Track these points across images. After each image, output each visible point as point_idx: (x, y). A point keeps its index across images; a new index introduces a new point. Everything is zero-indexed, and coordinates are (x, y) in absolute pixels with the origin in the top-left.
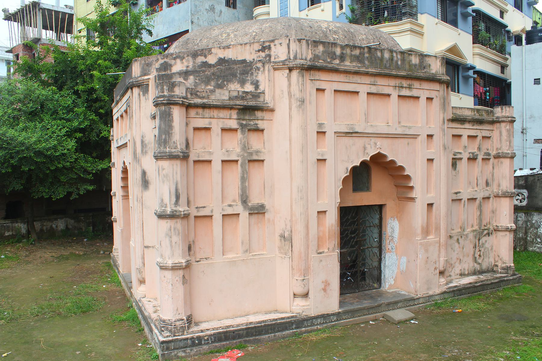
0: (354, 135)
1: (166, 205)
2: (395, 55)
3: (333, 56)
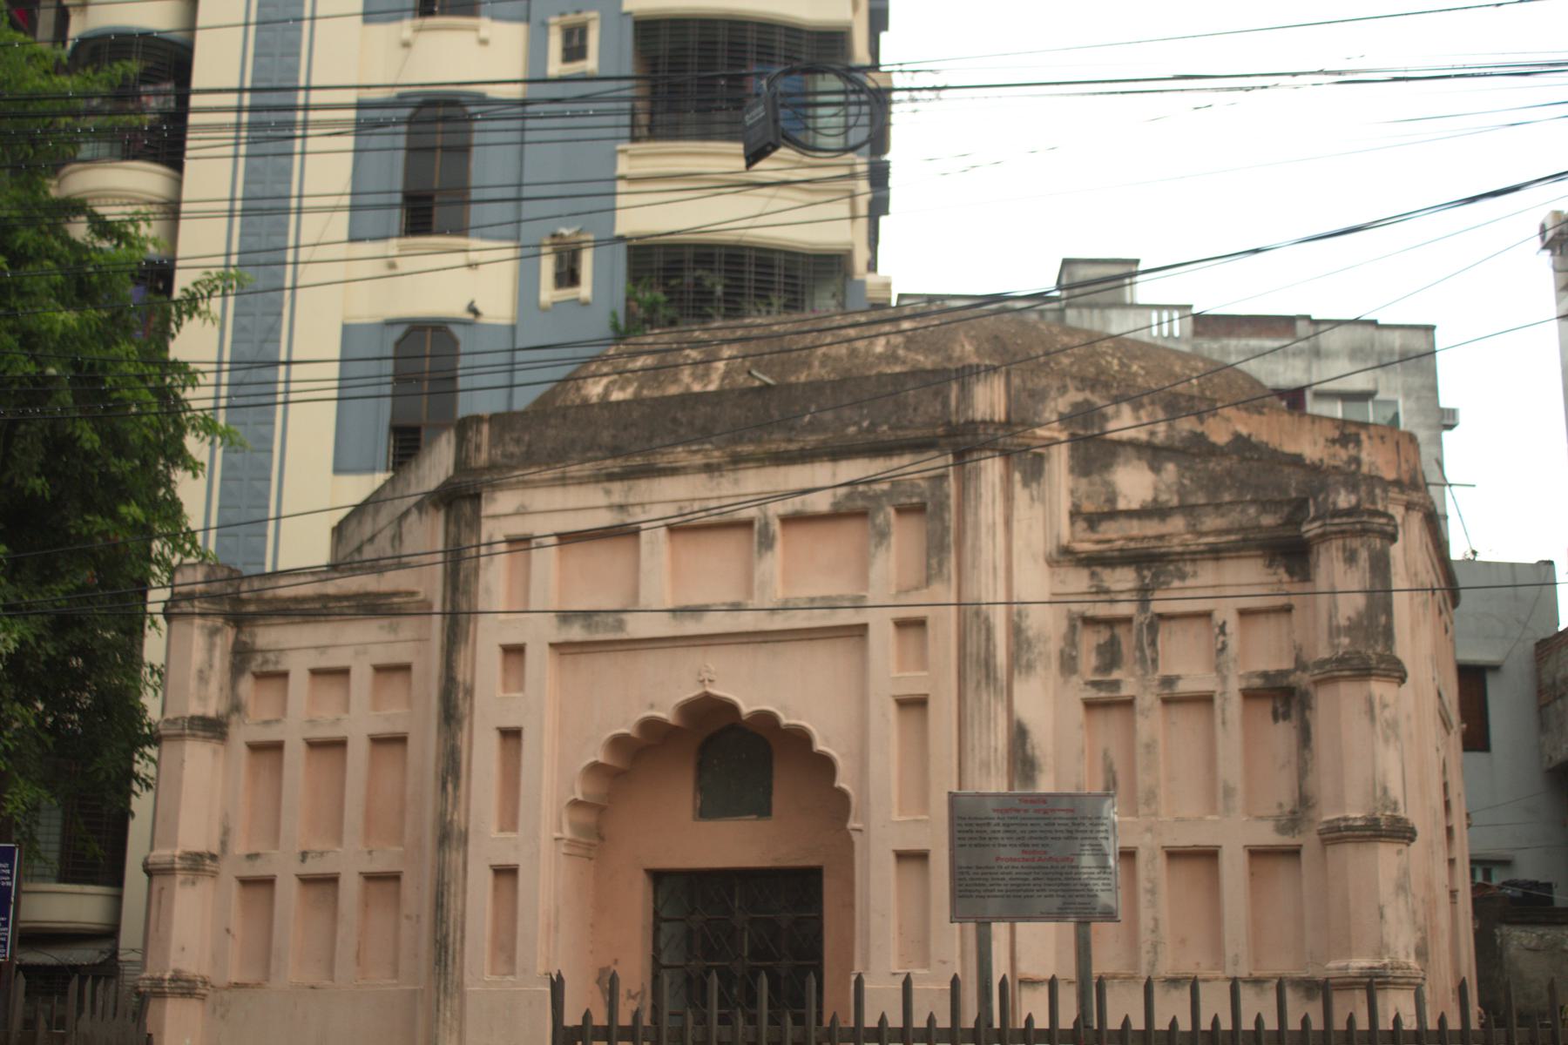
1: (1396, 803)
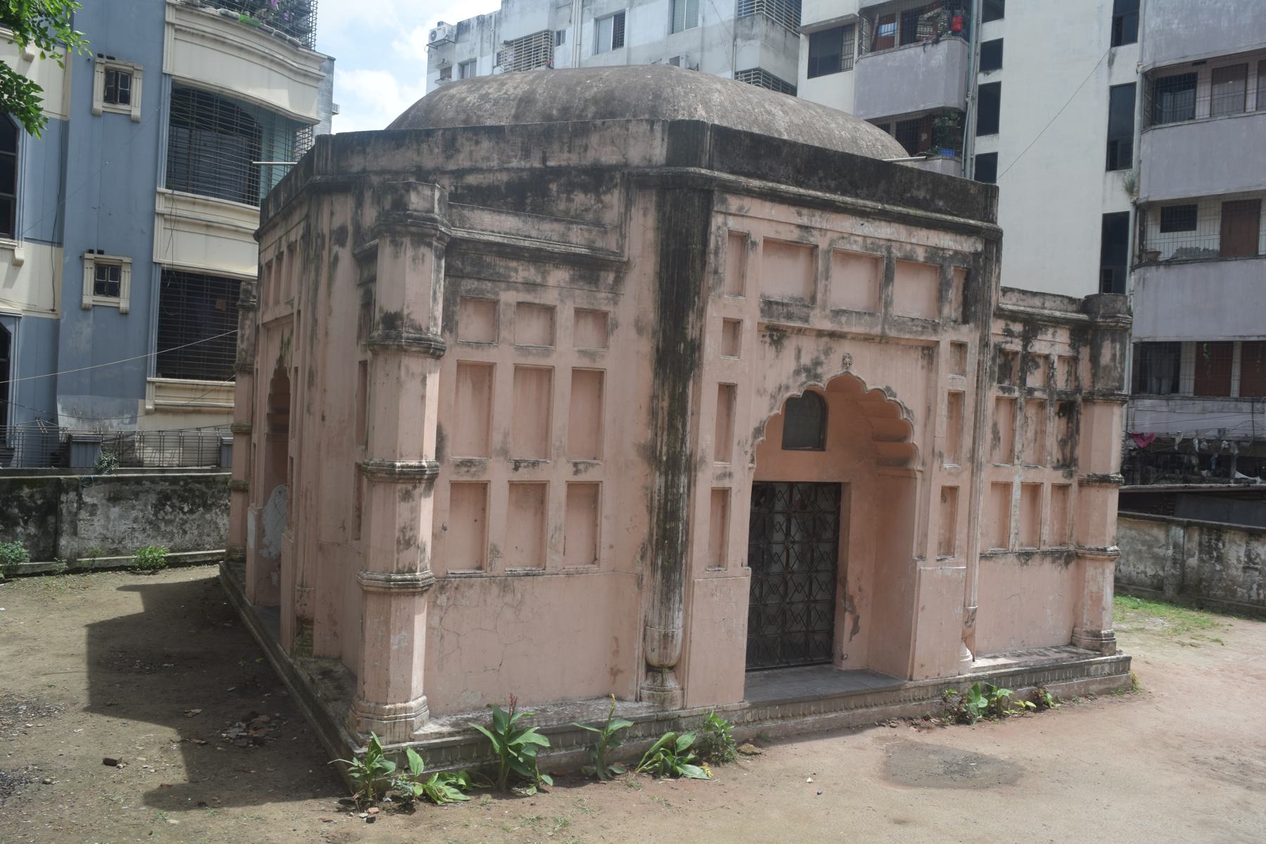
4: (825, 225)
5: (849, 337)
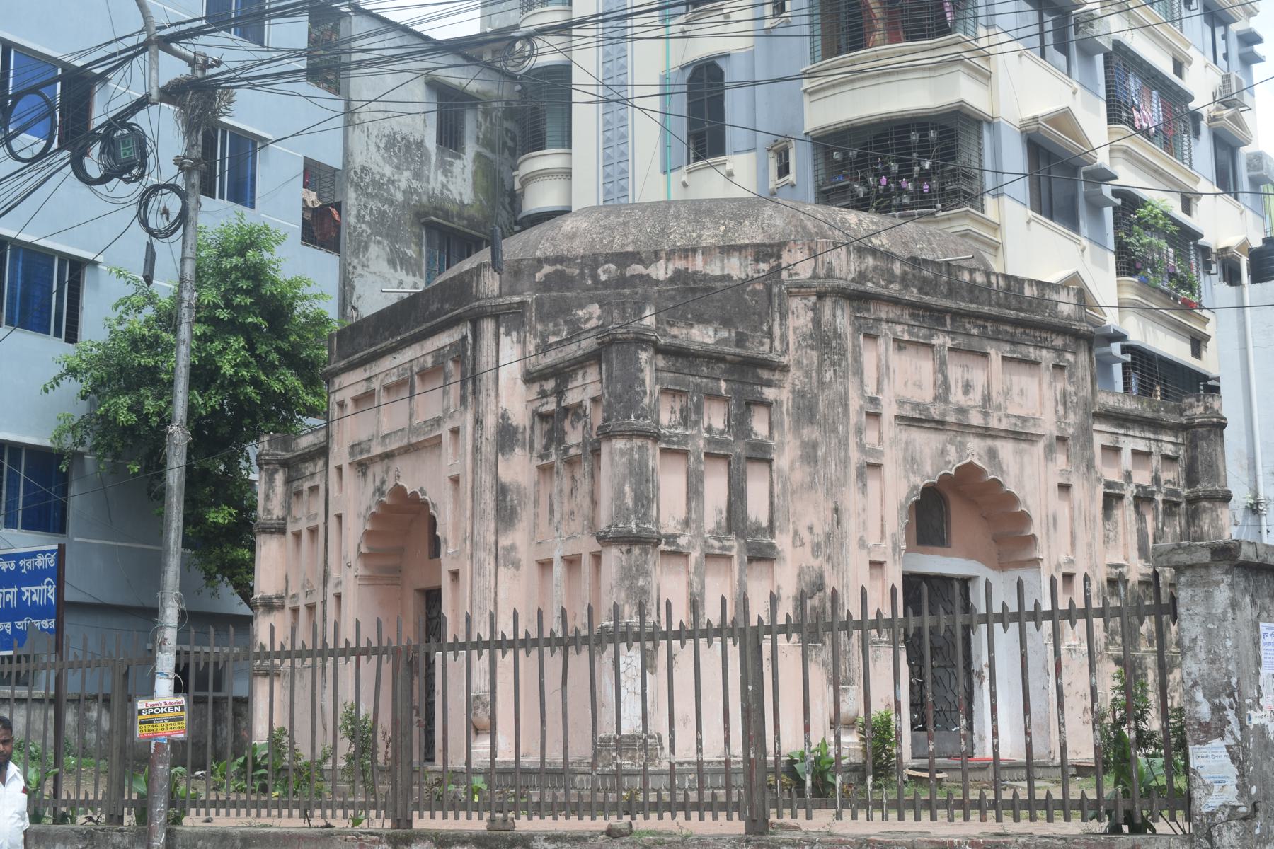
0: (926, 425)
2: (993, 279)
3: (891, 278)
4: (378, 371)
5: (396, 453)
